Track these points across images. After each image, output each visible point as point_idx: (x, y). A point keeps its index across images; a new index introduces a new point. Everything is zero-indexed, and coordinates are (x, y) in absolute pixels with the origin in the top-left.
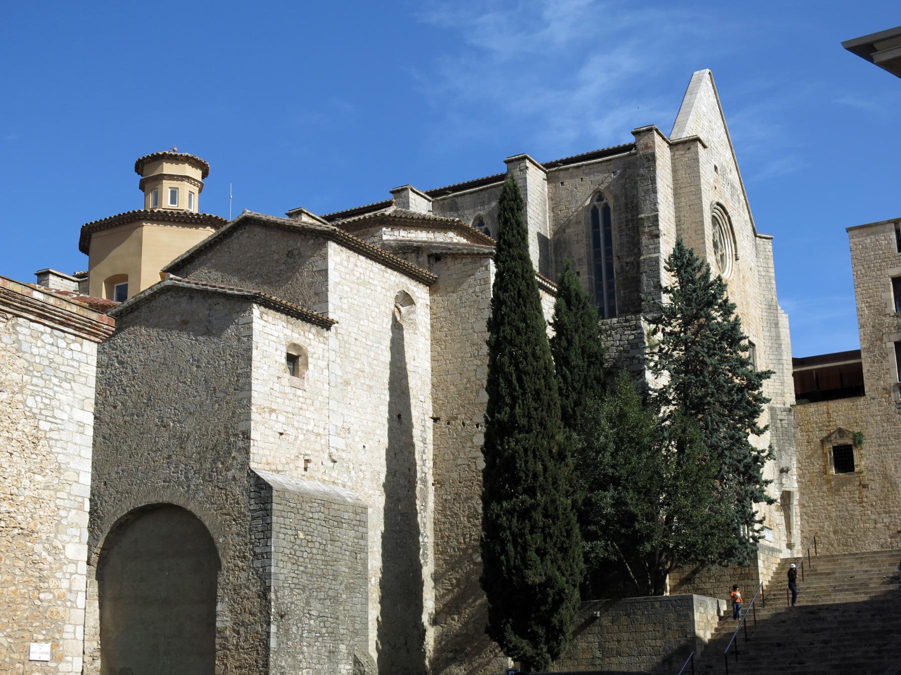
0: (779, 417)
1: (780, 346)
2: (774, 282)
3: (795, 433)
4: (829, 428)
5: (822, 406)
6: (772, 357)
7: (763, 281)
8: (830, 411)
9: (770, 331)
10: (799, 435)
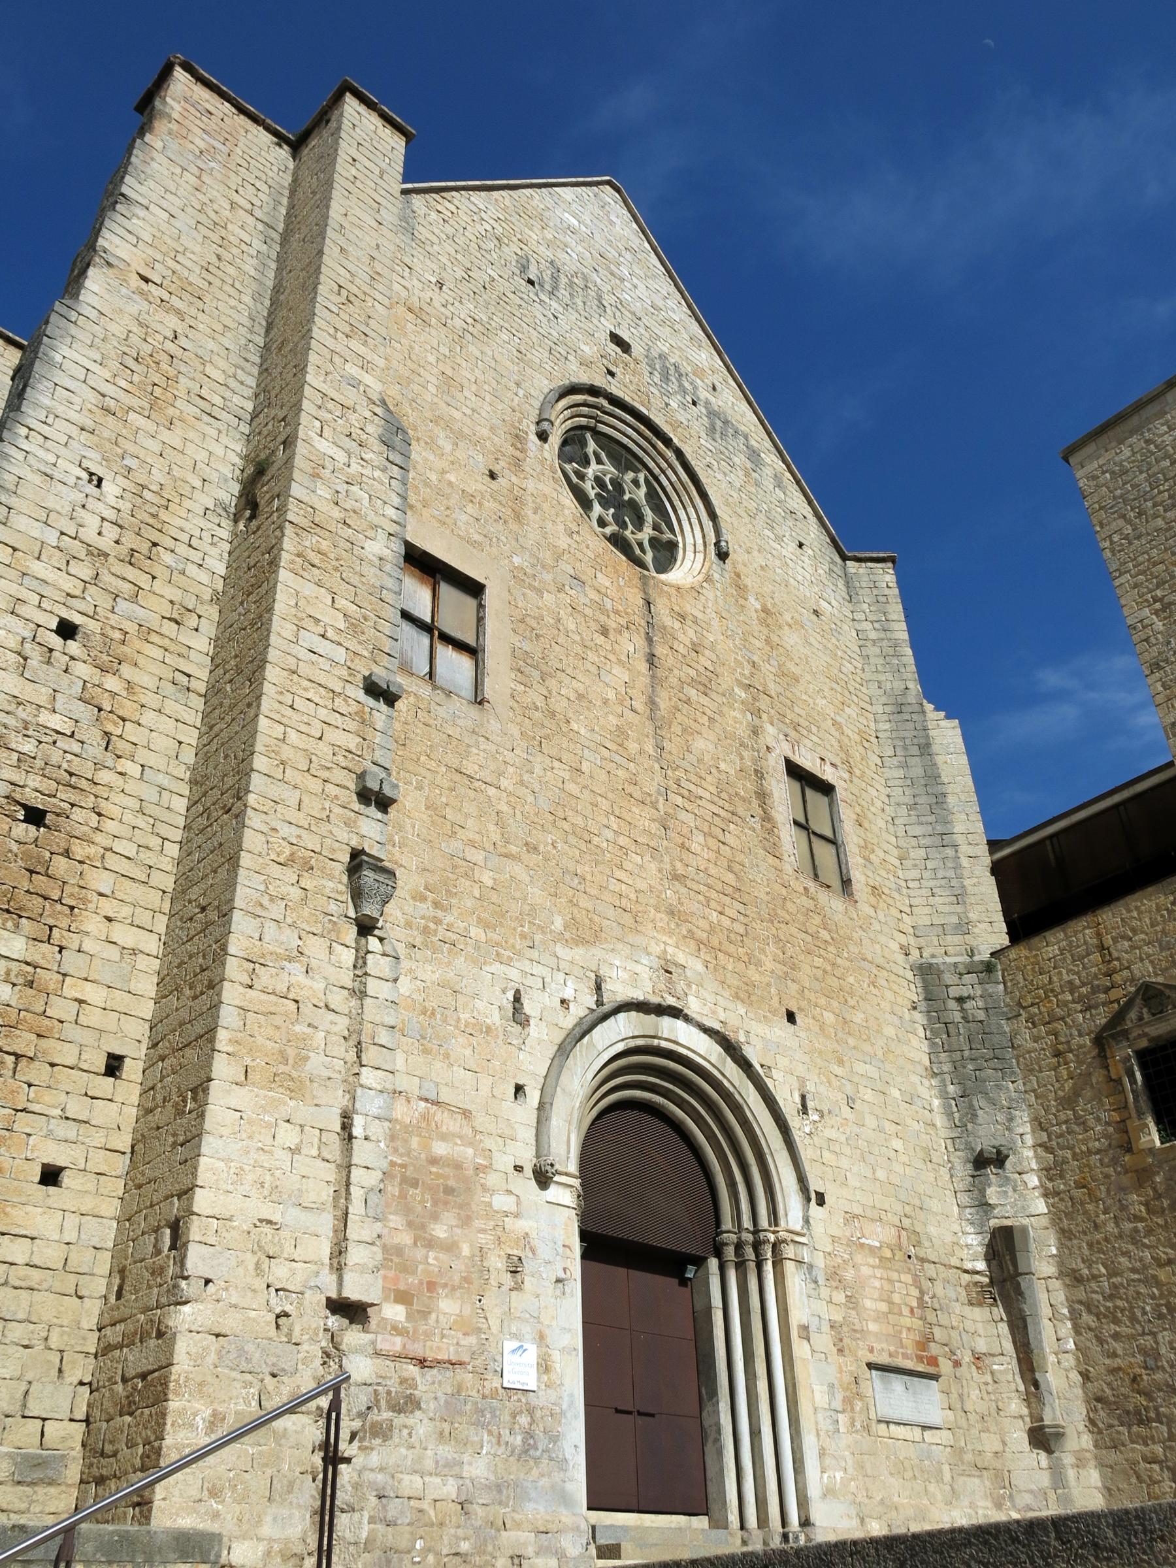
0: (954, 992)
1: (940, 800)
2: (909, 652)
3: (1015, 1033)
4: (1115, 994)
5: (1082, 931)
6: (918, 830)
7: (873, 651)
8: (1108, 940)
9: (904, 766)
10: (1025, 1038)
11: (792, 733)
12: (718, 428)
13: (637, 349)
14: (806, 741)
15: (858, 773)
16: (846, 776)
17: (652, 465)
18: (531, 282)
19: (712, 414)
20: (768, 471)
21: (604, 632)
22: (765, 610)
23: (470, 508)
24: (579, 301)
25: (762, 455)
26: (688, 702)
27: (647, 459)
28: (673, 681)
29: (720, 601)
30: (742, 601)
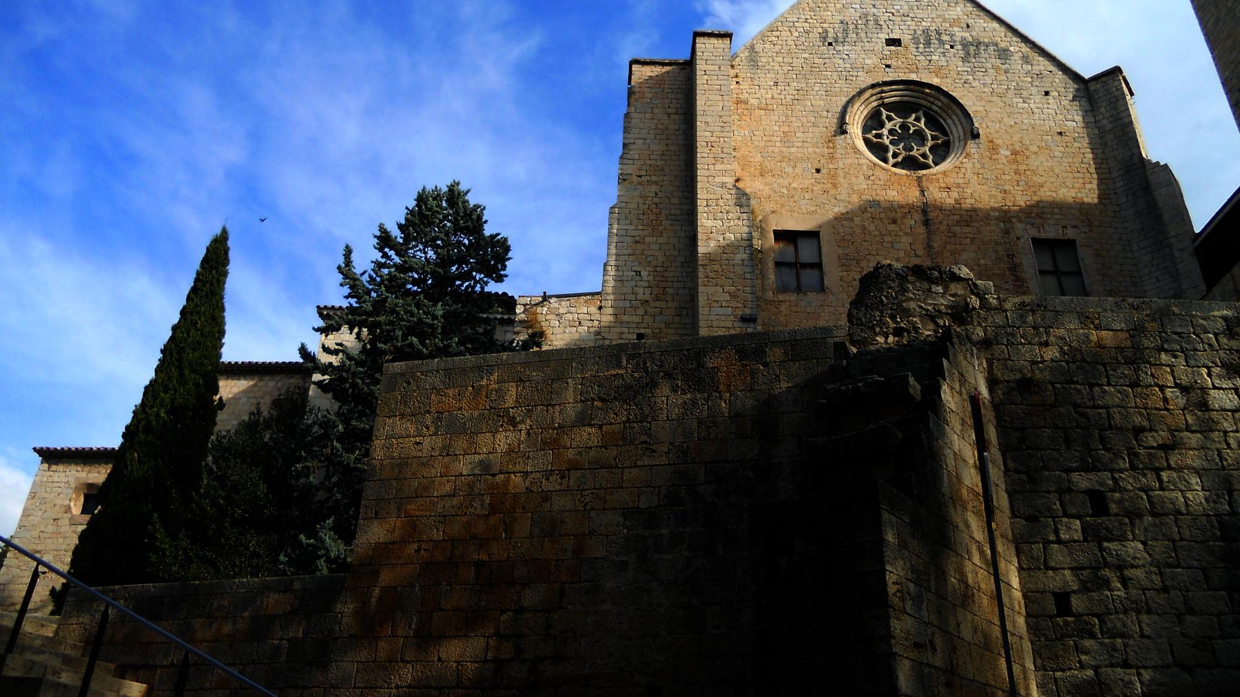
11: (1038, 221)
12: (972, 52)
13: (906, 39)
14: (1050, 221)
15: (1096, 223)
16: (1086, 229)
17: (925, 103)
18: (830, 44)
19: (965, 45)
20: (1017, 57)
21: (894, 222)
22: (1015, 153)
23: (807, 196)
24: (863, 35)
25: (1012, 49)
26: (955, 235)
27: (921, 101)
28: (943, 228)
29: (977, 165)
30: (995, 157)
